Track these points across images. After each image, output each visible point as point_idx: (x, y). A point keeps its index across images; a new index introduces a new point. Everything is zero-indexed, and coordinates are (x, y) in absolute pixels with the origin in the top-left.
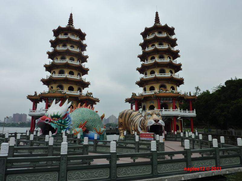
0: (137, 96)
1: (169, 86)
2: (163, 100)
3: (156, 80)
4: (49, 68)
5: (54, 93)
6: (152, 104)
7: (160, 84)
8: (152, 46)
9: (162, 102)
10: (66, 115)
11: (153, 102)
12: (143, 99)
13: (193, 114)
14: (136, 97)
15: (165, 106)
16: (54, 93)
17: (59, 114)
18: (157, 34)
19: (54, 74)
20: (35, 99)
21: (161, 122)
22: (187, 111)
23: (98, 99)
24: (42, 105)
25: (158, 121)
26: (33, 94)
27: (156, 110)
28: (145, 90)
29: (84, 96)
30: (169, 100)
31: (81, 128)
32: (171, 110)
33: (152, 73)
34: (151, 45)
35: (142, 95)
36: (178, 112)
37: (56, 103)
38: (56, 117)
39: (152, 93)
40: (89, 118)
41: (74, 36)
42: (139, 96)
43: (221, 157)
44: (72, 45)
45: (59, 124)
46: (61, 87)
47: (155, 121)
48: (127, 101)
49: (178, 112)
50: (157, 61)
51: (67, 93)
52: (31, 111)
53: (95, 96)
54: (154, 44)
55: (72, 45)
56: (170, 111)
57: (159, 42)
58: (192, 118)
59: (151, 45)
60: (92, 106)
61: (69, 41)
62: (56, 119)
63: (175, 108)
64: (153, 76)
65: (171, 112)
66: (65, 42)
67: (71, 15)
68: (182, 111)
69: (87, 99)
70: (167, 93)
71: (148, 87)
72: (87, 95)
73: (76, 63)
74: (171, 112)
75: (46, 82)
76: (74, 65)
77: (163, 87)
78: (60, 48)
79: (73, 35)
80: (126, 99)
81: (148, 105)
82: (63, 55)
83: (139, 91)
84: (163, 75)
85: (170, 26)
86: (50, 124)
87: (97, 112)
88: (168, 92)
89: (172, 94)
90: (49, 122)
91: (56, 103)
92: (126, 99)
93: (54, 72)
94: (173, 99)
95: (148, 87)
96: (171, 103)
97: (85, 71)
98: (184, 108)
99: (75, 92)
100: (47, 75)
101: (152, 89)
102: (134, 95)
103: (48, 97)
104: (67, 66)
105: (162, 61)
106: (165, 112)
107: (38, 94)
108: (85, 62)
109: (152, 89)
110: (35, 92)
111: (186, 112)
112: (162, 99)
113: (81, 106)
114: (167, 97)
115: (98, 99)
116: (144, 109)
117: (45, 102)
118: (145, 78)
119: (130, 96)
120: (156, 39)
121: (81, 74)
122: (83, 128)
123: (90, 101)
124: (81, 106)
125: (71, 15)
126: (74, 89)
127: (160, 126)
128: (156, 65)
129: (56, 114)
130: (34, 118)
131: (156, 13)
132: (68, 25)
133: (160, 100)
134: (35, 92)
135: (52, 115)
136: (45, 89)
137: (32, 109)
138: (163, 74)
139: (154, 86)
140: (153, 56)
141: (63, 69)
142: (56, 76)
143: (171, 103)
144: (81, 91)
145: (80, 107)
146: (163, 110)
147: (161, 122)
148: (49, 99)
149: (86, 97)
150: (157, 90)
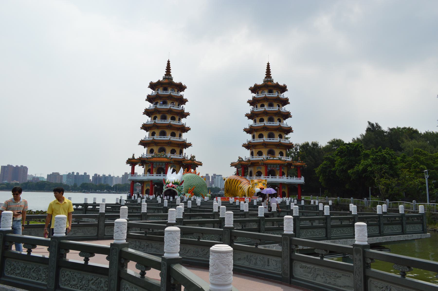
3: (265, 145)
5: (159, 157)
6: (259, 170)
9: (269, 169)
11: (261, 168)
13: (302, 180)
14: (243, 162)
15: (271, 173)
16: (159, 157)
22: (295, 178)
25: (263, 189)
27: (262, 177)
29: (188, 160)
32: (278, 177)
33: (261, 136)
35: (249, 160)
36: (285, 180)
39: (261, 158)
42: (246, 162)
43: (333, 227)
46: (162, 150)
47: (261, 189)
48: (232, 165)
49: (285, 180)
50: (266, 124)
51: (172, 157)
53: (197, 159)
54: (264, 103)
57: (269, 99)
58: (300, 185)
60: (195, 169)
63: (282, 174)
65: (278, 179)
67: (169, 61)
68: (289, 178)
69: (191, 164)
71: (255, 151)
72: (191, 158)
74: (278, 179)
75: (143, 143)
76: (177, 126)
77: (271, 153)
79: (173, 90)
81: (254, 170)
83: (246, 154)
85: (281, 84)
88: (275, 158)
89: (279, 162)
96: (278, 170)
98: (291, 175)
101: (260, 154)
102: (240, 160)
106: (271, 179)
107: (136, 157)
110: (134, 155)
114: (274, 164)
116: (251, 175)
119: (236, 160)
122: (191, 194)
125: (169, 61)
129: (176, 181)
130: (134, 182)
132: (165, 75)
134: (134, 155)
135: (174, 182)
139: (262, 151)
141: (165, 130)
143: (278, 170)
146: (270, 177)
148: (154, 164)
149: (189, 161)
150: (264, 156)
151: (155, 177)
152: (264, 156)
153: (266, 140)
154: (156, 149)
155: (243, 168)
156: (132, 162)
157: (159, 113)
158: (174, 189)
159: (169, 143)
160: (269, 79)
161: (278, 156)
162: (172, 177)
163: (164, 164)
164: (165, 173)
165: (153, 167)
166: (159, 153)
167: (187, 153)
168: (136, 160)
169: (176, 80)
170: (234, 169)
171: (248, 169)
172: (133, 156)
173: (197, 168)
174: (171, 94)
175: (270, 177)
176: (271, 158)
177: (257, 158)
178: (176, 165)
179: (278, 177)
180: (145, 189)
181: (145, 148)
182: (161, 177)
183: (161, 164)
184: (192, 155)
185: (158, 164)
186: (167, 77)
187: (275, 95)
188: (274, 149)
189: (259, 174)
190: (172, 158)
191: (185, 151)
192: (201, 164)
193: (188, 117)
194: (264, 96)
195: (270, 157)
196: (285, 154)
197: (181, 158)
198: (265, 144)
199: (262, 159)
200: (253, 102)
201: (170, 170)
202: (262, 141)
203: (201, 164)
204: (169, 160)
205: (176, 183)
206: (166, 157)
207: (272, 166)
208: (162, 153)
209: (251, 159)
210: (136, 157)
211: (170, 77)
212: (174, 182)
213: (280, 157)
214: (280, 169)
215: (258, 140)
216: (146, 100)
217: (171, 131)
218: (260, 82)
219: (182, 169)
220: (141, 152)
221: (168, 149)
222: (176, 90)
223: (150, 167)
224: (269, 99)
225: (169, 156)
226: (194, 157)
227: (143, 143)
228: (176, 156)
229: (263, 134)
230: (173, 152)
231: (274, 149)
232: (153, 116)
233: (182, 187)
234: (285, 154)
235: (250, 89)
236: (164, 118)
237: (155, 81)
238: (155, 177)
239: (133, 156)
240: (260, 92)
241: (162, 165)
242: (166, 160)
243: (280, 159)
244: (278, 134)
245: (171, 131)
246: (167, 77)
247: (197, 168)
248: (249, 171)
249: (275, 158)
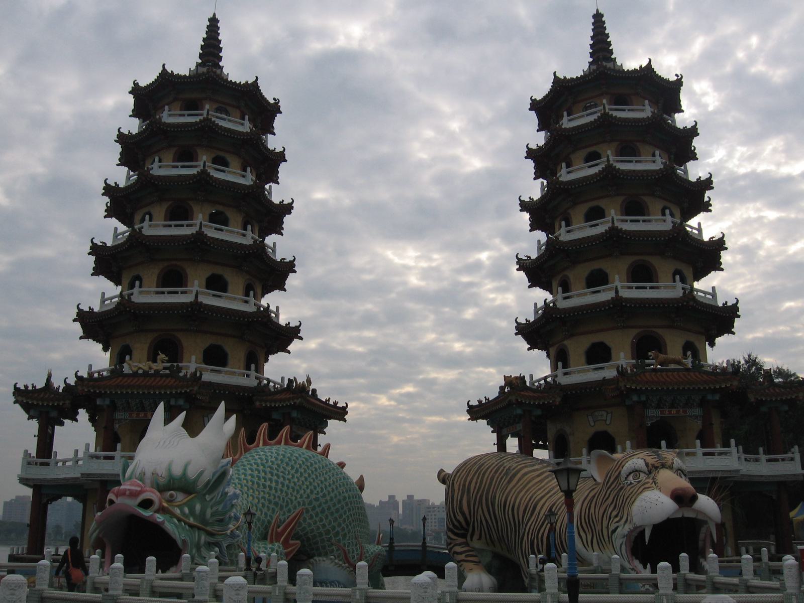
2: (658, 406)
3: (619, 311)
4: (106, 261)
6: (600, 427)
7: (634, 332)
8: (587, 161)
10: (221, 477)
17: (192, 474)
19: (136, 290)
20: (45, 405)
22: (763, 457)
24: (76, 436)
26: (40, 385)
28: (560, 359)
31: (276, 544)
32: (699, 451)
34: (583, 153)
37: (168, 420)
38: (177, 484)
40: (313, 496)
41: (227, 113)
45: (192, 520)
48: (475, 412)
52: (29, 463)
56: (694, 454)
59: (583, 153)
61: (207, 133)
62: (180, 497)
64: (605, 295)
66: (184, 143)
70: (670, 370)
73: (235, 234)
78: (162, 168)
86: (159, 518)
87: (342, 465)
90: (157, 511)
91: (168, 420)
93: (138, 278)
95: (577, 348)
97: (276, 274)
99: (233, 373)
100: (103, 294)
101: (598, 354)
102: (514, 385)
104: (199, 247)
108: (273, 235)
111: (757, 460)
113: (272, 434)
117: (92, 419)
118: (563, 304)
120: (606, 128)
121: (259, 291)
122: (286, 544)
123: (305, 412)
126: (230, 361)
128: (615, 242)
129: (177, 471)
131: (594, 16)
136: (97, 357)
137: (34, 454)
138: (648, 284)
139: (608, 343)
142: (148, 295)
144: (259, 369)
145: (265, 444)
158: (146, 513)
159: (195, 315)
188: (660, 331)
192: (340, 413)
197: (251, 382)
203: (340, 413)
209: (564, 380)
231: (660, 331)
236: (179, 213)
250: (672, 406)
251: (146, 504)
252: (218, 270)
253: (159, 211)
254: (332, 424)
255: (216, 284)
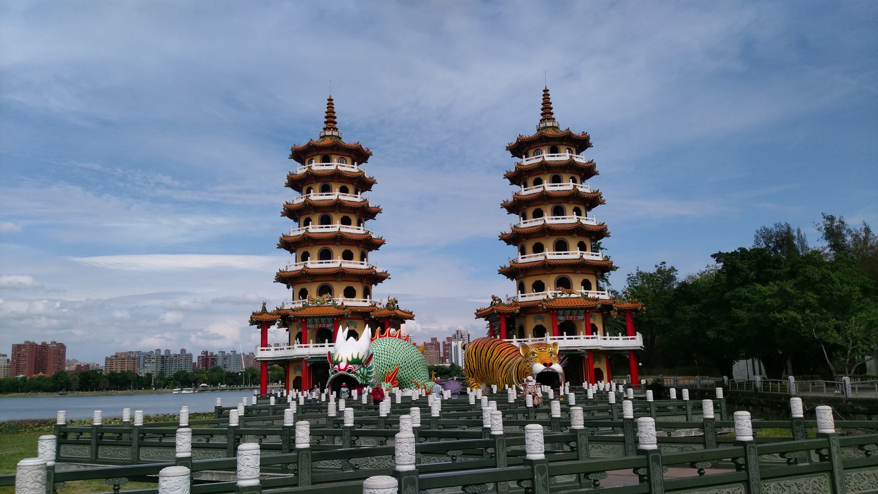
0: (504, 304)
1: (576, 282)
2: (564, 315)
6: (539, 322)
9: (562, 318)
11: (542, 319)
12: (518, 311)
13: (636, 342)
14: (501, 308)
15: (569, 329)
18: (547, 157)
21: (557, 367)
22: (620, 337)
23: (411, 313)
25: (551, 364)
27: (548, 339)
28: (521, 288)
30: (577, 315)
32: (582, 336)
33: (538, 248)
35: (516, 303)
36: (601, 341)
39: (540, 297)
42: (508, 306)
44: (344, 185)
47: (545, 364)
48: (480, 314)
50: (548, 222)
51: (346, 304)
53: (403, 306)
54: (541, 177)
55: (344, 185)
58: (633, 352)
62: (357, 366)
63: (592, 330)
64: (542, 258)
65: (582, 342)
68: (608, 337)
69: (390, 317)
71: (529, 283)
74: (582, 342)
75: (284, 278)
76: (355, 237)
77: (564, 284)
80: (478, 311)
82: (325, 213)
84: (562, 256)
85: (577, 132)
88: (572, 296)
92: (478, 311)
94: (585, 312)
98: (613, 329)
103: (309, 317)
105: (561, 221)
106: (566, 342)
107: (270, 309)
109: (539, 287)
112: (561, 312)
115: (411, 313)
116: (522, 335)
119: (486, 303)
124: (382, 332)
127: (555, 374)
129: (355, 357)
133: (557, 315)
135: (350, 359)
140: (537, 207)
142: (314, 264)
147: (557, 367)
148: (309, 320)
150: (550, 292)
151: (312, 350)
152: (550, 292)
153: (549, 257)
154: (313, 290)
155: (504, 320)
156: (262, 321)
157: (316, 212)
160: (549, 124)
161: (578, 290)
162: (346, 349)
163: (329, 320)
164: (332, 338)
165: (305, 329)
166: (320, 299)
167: (380, 294)
168: (270, 314)
169: (348, 140)
170: (483, 325)
171: (514, 324)
172: (264, 309)
173: (402, 325)
174: (339, 168)
175: (565, 337)
176: (564, 296)
177: (532, 297)
178: (356, 321)
179: (582, 336)
180: (292, 378)
181: (288, 287)
182: (323, 350)
183: (323, 320)
184: (391, 298)
185: (316, 320)
186: (328, 133)
187: (564, 156)
189: (539, 332)
190: (347, 306)
191: (375, 289)
193: (378, 216)
194: (540, 160)
195: (562, 294)
196: (594, 286)
198: (550, 265)
199: (545, 297)
200: (517, 177)
201: (342, 333)
202: (542, 258)
204: (341, 312)
205: (357, 362)
206: (334, 305)
207: (568, 312)
208: (326, 297)
209: (521, 300)
210: (270, 309)
211: (335, 133)
212: (350, 359)
213: (583, 291)
214: (587, 320)
215: (532, 258)
216: (287, 185)
217: (343, 249)
218: (530, 131)
219: (367, 331)
220: (283, 297)
221: (339, 289)
222: (349, 160)
223: (300, 330)
224: (550, 168)
225: (339, 304)
226: (396, 302)
227: (284, 278)
228: (357, 302)
229: (543, 243)
230: (350, 293)
232: (302, 220)
233: (371, 368)
234: (594, 286)
235: (508, 148)
237: (302, 143)
238: (312, 350)
239: (264, 309)
240: (531, 152)
241: (327, 323)
242: (333, 312)
243: (585, 297)
244: (577, 242)
245: (343, 249)
246: (328, 133)
247: (402, 325)
248: (517, 326)
249: (572, 296)
250: (571, 315)
251: (349, 371)
252: (348, 248)
253: (316, 218)
254: (407, 321)
255: (348, 256)
